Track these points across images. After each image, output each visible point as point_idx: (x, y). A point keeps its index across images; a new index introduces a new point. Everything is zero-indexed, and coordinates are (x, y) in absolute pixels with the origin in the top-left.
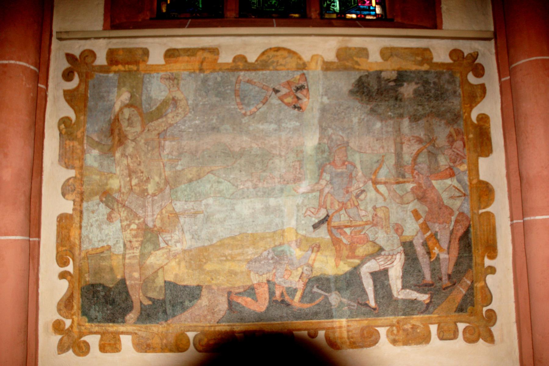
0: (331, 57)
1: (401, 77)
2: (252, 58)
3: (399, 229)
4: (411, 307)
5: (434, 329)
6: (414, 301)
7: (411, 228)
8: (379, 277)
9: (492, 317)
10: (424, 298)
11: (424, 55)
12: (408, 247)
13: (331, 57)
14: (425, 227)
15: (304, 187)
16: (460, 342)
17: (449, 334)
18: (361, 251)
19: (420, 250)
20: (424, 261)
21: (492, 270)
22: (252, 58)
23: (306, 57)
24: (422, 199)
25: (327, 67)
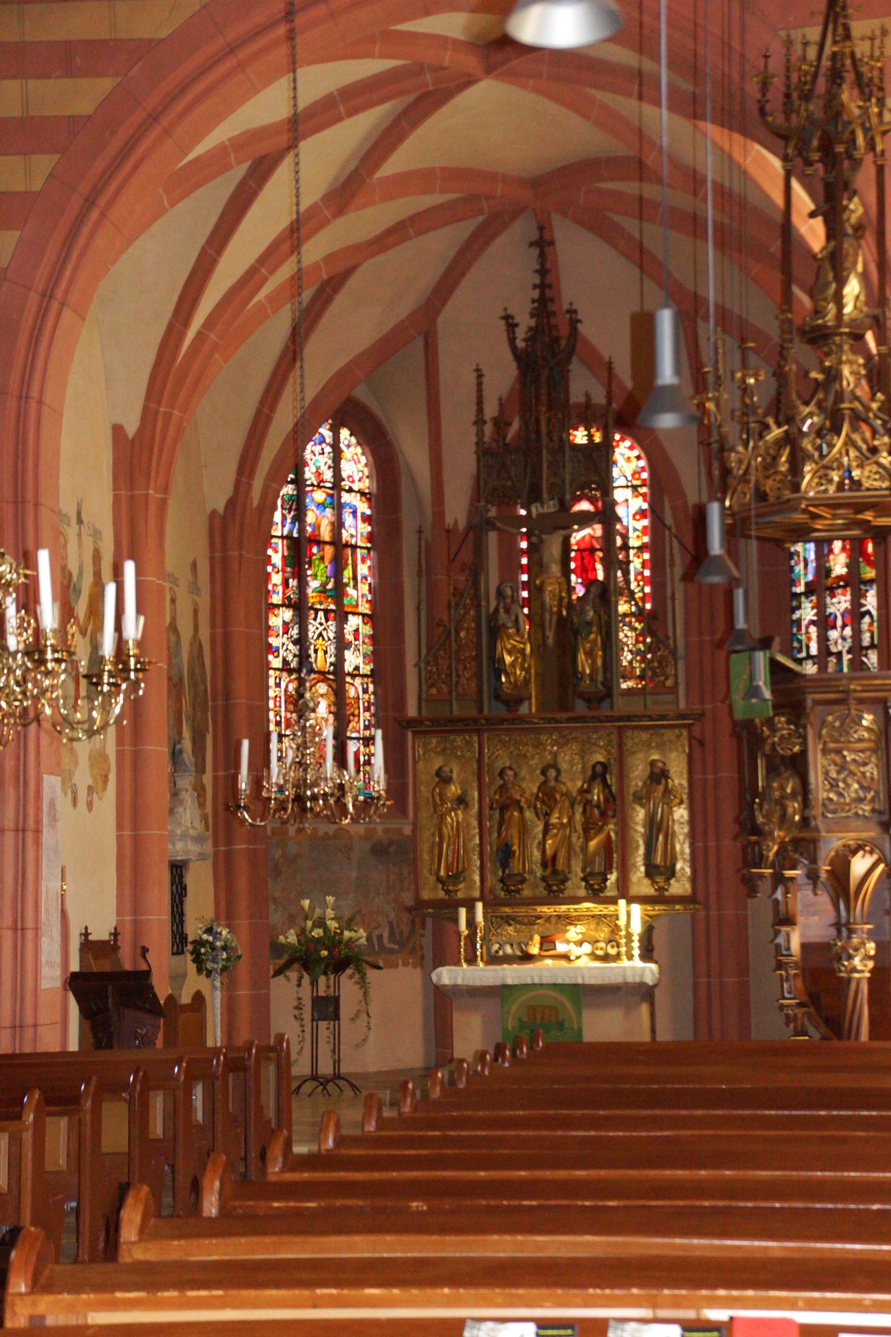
0: (362, 832)
1: (391, 843)
2: (331, 833)
3: (387, 916)
4: (392, 951)
5: (400, 961)
6: (393, 949)
7: (392, 915)
8: (380, 937)
9: (423, 957)
10: (396, 947)
11: (399, 831)
12: (391, 924)
13: (362, 832)
14: (397, 915)
15: (351, 896)
16: (410, 968)
17: (405, 964)
18: (373, 925)
19: (395, 926)
20: (397, 931)
21: (423, 935)
22: (331, 833)
23: (352, 833)
24: (396, 902)
25: (361, 838)
